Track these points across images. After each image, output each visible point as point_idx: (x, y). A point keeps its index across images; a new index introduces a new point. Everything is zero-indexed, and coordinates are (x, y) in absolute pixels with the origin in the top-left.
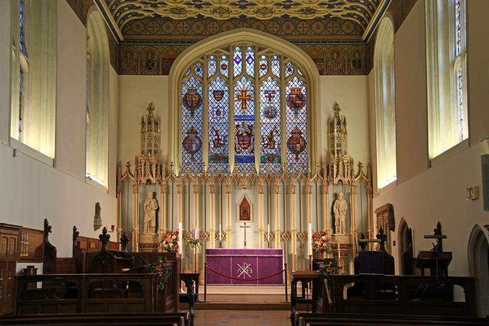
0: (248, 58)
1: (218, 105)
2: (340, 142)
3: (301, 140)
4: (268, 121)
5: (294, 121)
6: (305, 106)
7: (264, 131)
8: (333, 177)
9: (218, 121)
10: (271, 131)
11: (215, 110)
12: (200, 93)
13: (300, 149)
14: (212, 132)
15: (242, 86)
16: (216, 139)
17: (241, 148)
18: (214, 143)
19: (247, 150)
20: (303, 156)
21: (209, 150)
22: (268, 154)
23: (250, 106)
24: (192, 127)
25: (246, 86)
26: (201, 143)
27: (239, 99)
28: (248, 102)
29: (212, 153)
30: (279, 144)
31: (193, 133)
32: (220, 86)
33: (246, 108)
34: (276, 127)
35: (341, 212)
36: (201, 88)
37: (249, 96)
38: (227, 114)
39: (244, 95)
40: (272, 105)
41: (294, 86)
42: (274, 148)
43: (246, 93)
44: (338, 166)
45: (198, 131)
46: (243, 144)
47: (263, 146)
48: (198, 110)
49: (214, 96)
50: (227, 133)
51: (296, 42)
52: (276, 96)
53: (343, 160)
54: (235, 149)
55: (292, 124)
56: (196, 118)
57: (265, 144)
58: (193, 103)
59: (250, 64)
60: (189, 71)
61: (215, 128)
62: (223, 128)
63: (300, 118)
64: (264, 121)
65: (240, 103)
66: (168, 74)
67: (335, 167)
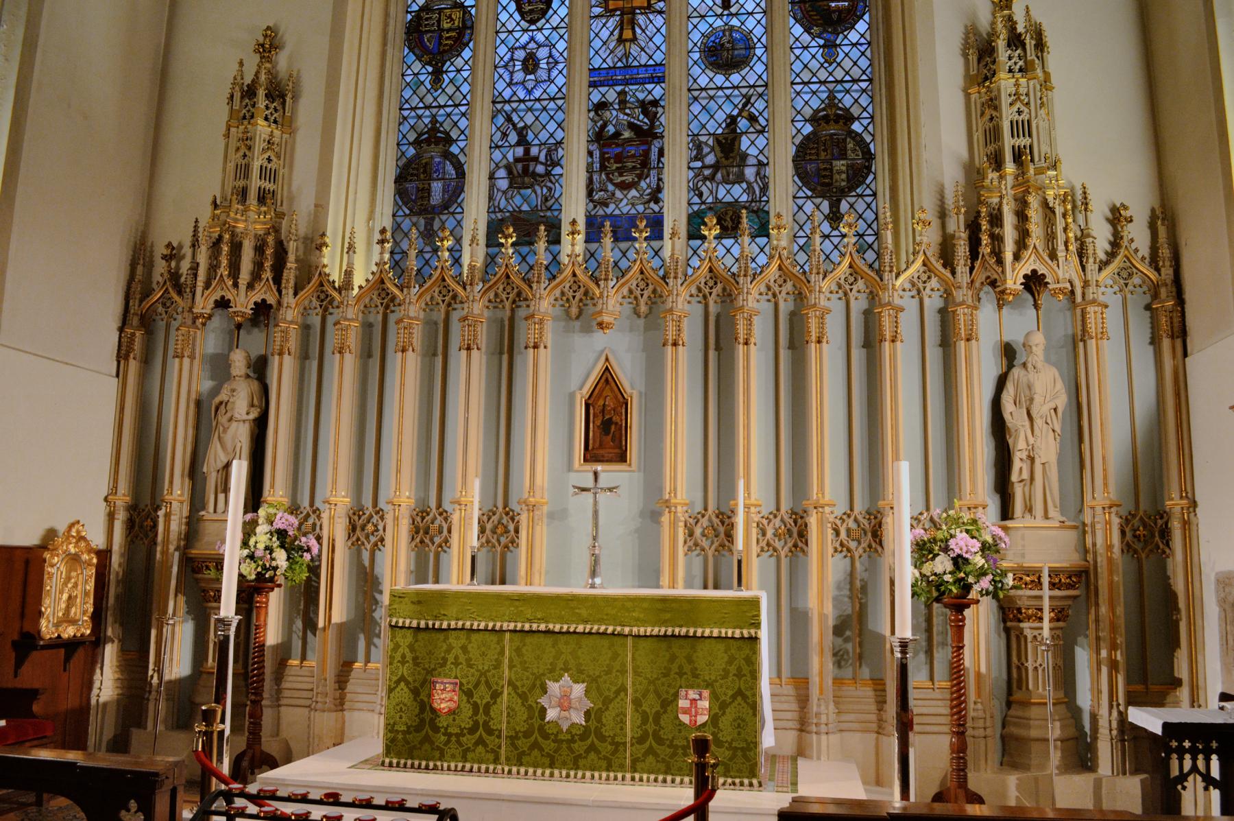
1: (532, 39)
2: (1025, 117)
3: (850, 145)
4: (719, 79)
5: (823, 75)
6: (866, 17)
7: (704, 118)
8: (1000, 262)
9: (530, 92)
10: (730, 116)
11: (520, 54)
13: (848, 180)
14: (505, 135)
16: (517, 160)
17: (611, 187)
19: (633, 193)
20: (860, 206)
21: (491, 198)
23: (651, 30)
26: (461, 174)
27: (606, 9)
28: (641, 19)
29: (501, 211)
33: (634, 39)
34: (748, 102)
35: (1039, 422)
38: (560, 66)
40: (735, 22)
42: (740, 178)
44: (1022, 216)
45: (454, 134)
47: (696, 176)
48: (459, 62)
50: (559, 135)
53: (1041, 189)
54: (590, 193)
55: (814, 87)
56: (450, 90)
58: (441, 37)
61: (515, 118)
62: (544, 117)
63: (847, 64)
64: (703, 81)
65: (612, 23)
67: (1009, 220)
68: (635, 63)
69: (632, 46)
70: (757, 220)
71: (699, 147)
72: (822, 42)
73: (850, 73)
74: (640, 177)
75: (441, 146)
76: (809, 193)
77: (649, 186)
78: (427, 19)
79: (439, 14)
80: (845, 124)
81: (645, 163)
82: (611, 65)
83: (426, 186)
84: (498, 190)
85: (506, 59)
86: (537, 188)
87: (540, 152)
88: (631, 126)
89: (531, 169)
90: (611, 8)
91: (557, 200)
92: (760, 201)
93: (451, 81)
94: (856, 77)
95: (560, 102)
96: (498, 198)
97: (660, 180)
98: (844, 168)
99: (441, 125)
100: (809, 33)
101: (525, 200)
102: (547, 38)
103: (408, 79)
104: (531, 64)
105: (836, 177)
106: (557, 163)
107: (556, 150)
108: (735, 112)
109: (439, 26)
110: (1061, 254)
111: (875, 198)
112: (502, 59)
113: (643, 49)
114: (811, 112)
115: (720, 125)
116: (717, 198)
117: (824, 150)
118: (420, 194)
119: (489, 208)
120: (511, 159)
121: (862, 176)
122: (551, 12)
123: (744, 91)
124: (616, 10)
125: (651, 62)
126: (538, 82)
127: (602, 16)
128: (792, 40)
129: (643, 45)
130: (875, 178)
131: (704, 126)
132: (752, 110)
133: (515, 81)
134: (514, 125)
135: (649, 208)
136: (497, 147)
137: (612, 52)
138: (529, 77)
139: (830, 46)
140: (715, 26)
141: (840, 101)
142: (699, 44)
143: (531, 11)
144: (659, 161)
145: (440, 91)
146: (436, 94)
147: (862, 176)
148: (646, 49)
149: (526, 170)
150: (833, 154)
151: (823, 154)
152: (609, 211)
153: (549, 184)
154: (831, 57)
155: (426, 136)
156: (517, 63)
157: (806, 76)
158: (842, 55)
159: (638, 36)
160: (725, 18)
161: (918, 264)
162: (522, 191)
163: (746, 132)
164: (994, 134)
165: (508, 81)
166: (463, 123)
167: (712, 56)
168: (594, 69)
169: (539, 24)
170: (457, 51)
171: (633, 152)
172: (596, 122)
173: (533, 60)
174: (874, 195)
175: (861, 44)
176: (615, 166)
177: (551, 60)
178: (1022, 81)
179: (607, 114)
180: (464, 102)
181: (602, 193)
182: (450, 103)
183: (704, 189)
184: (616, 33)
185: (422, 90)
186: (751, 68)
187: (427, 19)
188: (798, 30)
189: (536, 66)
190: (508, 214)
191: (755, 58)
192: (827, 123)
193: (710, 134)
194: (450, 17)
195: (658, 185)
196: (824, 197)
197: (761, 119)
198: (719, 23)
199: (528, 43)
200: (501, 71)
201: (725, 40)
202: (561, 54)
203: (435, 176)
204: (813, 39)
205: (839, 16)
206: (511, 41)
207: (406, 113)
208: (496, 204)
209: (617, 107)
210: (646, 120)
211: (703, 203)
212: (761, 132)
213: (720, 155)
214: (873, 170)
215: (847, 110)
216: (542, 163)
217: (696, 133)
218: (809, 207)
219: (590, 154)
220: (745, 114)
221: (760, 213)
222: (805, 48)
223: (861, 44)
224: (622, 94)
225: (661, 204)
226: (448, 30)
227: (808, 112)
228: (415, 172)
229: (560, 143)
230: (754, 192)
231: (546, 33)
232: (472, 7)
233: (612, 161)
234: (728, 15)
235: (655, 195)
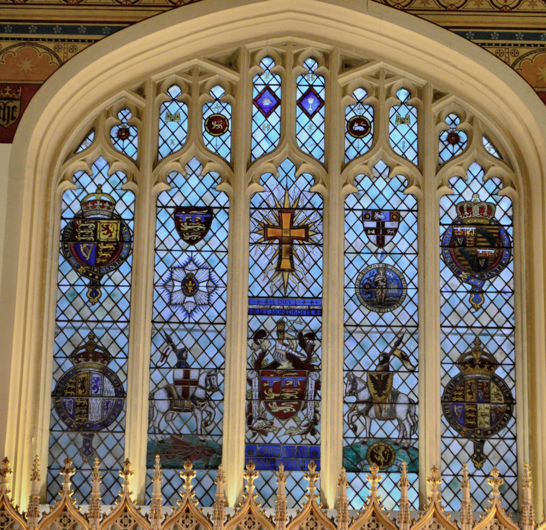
0: (305, 96)
1: (191, 260)
3: (494, 389)
4: (373, 317)
5: (470, 319)
6: (511, 265)
7: (358, 353)
9: (189, 314)
10: (383, 354)
11: (180, 275)
12: (127, 215)
13: (492, 423)
14: (165, 356)
15: (279, 193)
16: (177, 382)
17: (269, 416)
18: (170, 394)
19: (291, 423)
20: (502, 448)
21: (151, 419)
22: (370, 436)
23: (308, 262)
24: (92, 336)
25: (294, 192)
26: (121, 393)
27: (266, 237)
28: (299, 250)
29: (161, 433)
30: (411, 403)
31: (95, 359)
32: (201, 189)
33: (292, 270)
34: (400, 341)
36: (129, 198)
37: (306, 228)
38: (220, 291)
39: (286, 225)
40: (388, 260)
41: (468, 196)
42: (392, 416)
43: (293, 217)
45: (113, 351)
46: (279, 401)
47: (351, 410)
48: (117, 276)
49: (178, 227)
50: (219, 360)
51: (477, 36)
52: (402, 228)
54: (249, 421)
55: (462, 331)
56: (108, 305)
57: (358, 402)
58: (98, 248)
59: (310, 117)
60: (91, 137)
61: (175, 340)
62: (203, 342)
63: (492, 310)
64: (358, 317)
65: (271, 250)
66: (10, 140)
68: (293, 294)
69: (291, 276)
70: (407, 457)
71: (354, 382)
72: (469, 287)
73: (495, 319)
74: (297, 407)
75: (99, 362)
76: (456, 434)
77: (306, 417)
78: (83, 228)
79: (96, 224)
80: (489, 369)
81: (302, 396)
82: (270, 294)
83: (85, 402)
84: (158, 411)
85: (165, 278)
86: (197, 411)
87: (200, 375)
88: (290, 357)
89: (191, 393)
90: (269, 235)
91: (216, 425)
92: (411, 439)
93: (109, 295)
94: (500, 324)
95: (219, 327)
96: (158, 420)
97: (316, 412)
98: (488, 412)
99: (99, 340)
100: (458, 278)
101: (185, 422)
102: (206, 260)
103: (64, 289)
105: (480, 419)
106: (215, 389)
107: (216, 375)
108: (388, 350)
109: (95, 236)
111: (516, 441)
112: (161, 277)
113: (300, 281)
114: (459, 355)
115: (373, 362)
116: (370, 433)
117: (471, 393)
118: (78, 410)
119: (149, 429)
120: (171, 382)
121: (504, 420)
122: (210, 233)
123: (397, 330)
124: (274, 238)
125: (308, 295)
126: (198, 305)
127: (260, 243)
128: (442, 283)
129: (301, 276)
130: (515, 422)
131: (358, 362)
132: (404, 349)
133: (174, 302)
134: (174, 347)
135: (306, 439)
136: (157, 367)
137: (270, 280)
138: (188, 299)
140: (369, 263)
141: (485, 346)
142: (354, 281)
143: (190, 231)
144: (316, 393)
145: (98, 305)
146: (93, 308)
147: (504, 420)
148: (304, 281)
149: (185, 394)
150: (478, 397)
151: (469, 397)
152: (267, 439)
153: (209, 409)
154: (477, 303)
155: (83, 350)
156: (176, 283)
157: (454, 320)
158: (487, 301)
159: (296, 267)
160: (379, 256)
162: (183, 414)
163: (397, 371)
165: (167, 300)
166: (122, 340)
167: (368, 293)
168: (254, 297)
169: (200, 244)
170: (115, 265)
171: (291, 383)
172: (255, 350)
173: (193, 282)
174: (515, 438)
175: (505, 293)
176: (273, 395)
177: (210, 284)
179: (266, 344)
180: (123, 319)
181: (261, 421)
182: (108, 318)
183: (358, 423)
184: (275, 261)
185: (79, 303)
186: (404, 308)
187: (83, 228)
188: (448, 273)
189: (196, 288)
190: (168, 436)
191: (407, 299)
192: (473, 366)
193: (364, 371)
194: (107, 228)
195: (315, 417)
196: (468, 437)
197: (412, 359)
198: (373, 260)
199: (187, 264)
200: (161, 290)
201: (379, 278)
202: (221, 278)
203: (93, 392)
204: (461, 284)
205: (486, 263)
206: (170, 259)
207: (62, 325)
208: (156, 426)
209: (274, 335)
210: (303, 352)
211: (357, 437)
212: (412, 372)
213: (373, 391)
214: (514, 414)
215: (491, 355)
216: (201, 387)
217: (351, 368)
218: (455, 447)
219: (250, 381)
220: (397, 353)
221: (410, 450)
222: (454, 292)
223: (505, 293)
224: (280, 323)
225: (317, 435)
226: (105, 243)
227: (455, 355)
228: (72, 387)
230: (405, 430)
231: (206, 255)
232: (130, 220)
233: (271, 390)
234: (382, 253)
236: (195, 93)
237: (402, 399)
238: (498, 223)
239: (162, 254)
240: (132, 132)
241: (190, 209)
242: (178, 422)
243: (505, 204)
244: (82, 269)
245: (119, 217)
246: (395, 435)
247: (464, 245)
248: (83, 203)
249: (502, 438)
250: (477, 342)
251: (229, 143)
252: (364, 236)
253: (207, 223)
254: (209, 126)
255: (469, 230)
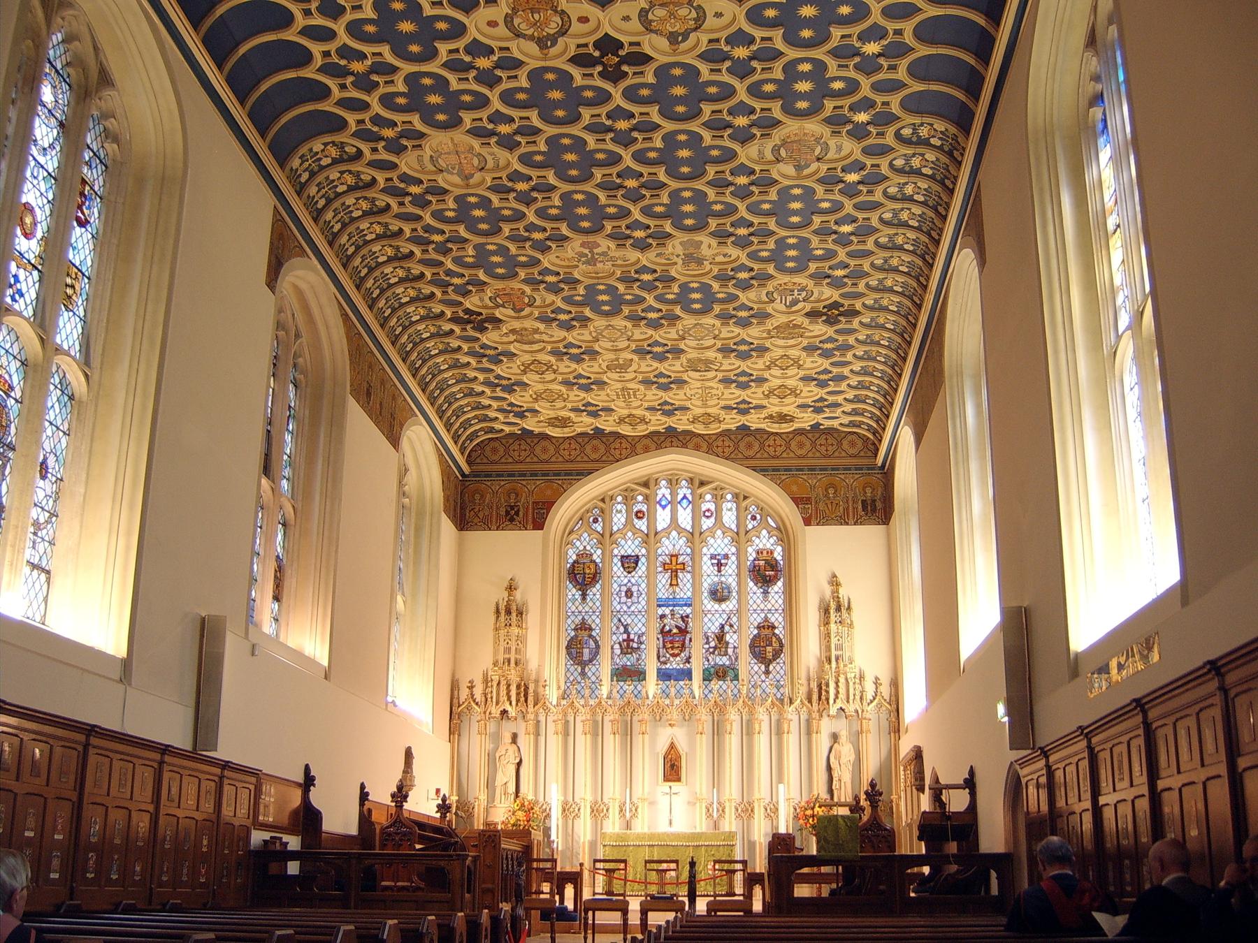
1: (629, 581)
2: (840, 642)
3: (774, 639)
4: (716, 606)
5: (762, 606)
6: (782, 579)
7: (710, 624)
9: (629, 608)
11: (624, 589)
12: (598, 561)
14: (618, 628)
15: (671, 547)
16: (624, 640)
17: (668, 656)
18: (621, 646)
19: (678, 658)
20: (778, 668)
21: (612, 658)
24: (583, 619)
25: (677, 547)
26: (598, 647)
27: (664, 569)
28: (680, 575)
30: (735, 647)
31: (585, 630)
32: (633, 547)
33: (677, 585)
34: (729, 618)
36: (599, 552)
37: (684, 564)
38: (643, 596)
39: (674, 563)
40: (723, 579)
41: (761, 546)
44: (837, 683)
46: (672, 648)
48: (594, 590)
49: (623, 565)
50: (644, 629)
51: (762, 470)
52: (729, 563)
53: (845, 673)
54: (658, 657)
56: (591, 604)
57: (710, 647)
60: (580, 522)
61: (622, 619)
64: (709, 607)
66: (542, 529)
74: (681, 651)
81: (683, 645)
88: (677, 627)
103: (570, 597)
104: (629, 594)
106: (641, 643)
108: (724, 622)
110: (851, 701)
131: (710, 628)
139: (766, 593)
143: (629, 567)
149: (628, 645)
152: (667, 666)
157: (755, 607)
161: (799, 701)
164: (828, 648)
169: (633, 573)
176: (670, 646)
178: (840, 627)
184: (669, 581)
188: (751, 584)
189: (632, 595)
197: (735, 626)
198: (716, 579)
200: (615, 596)
209: (670, 616)
212: (735, 632)
215: (773, 624)
218: (756, 668)
219: (658, 639)
227: (756, 624)
229: (643, 634)
235: (688, 661)
236: (629, 500)
237: (730, 646)
238: (775, 559)
239: (615, 579)
240: (600, 519)
241: (628, 557)
242: (625, 659)
243: (779, 549)
244: (578, 587)
245: (594, 561)
246: (727, 663)
247: (759, 570)
248: (577, 555)
249: (778, 663)
250: (766, 617)
251: (646, 523)
252: (711, 567)
253: (636, 563)
254: (636, 515)
255: (762, 563)
